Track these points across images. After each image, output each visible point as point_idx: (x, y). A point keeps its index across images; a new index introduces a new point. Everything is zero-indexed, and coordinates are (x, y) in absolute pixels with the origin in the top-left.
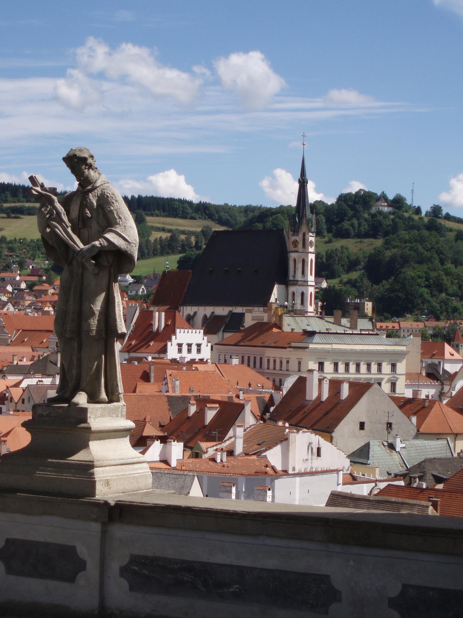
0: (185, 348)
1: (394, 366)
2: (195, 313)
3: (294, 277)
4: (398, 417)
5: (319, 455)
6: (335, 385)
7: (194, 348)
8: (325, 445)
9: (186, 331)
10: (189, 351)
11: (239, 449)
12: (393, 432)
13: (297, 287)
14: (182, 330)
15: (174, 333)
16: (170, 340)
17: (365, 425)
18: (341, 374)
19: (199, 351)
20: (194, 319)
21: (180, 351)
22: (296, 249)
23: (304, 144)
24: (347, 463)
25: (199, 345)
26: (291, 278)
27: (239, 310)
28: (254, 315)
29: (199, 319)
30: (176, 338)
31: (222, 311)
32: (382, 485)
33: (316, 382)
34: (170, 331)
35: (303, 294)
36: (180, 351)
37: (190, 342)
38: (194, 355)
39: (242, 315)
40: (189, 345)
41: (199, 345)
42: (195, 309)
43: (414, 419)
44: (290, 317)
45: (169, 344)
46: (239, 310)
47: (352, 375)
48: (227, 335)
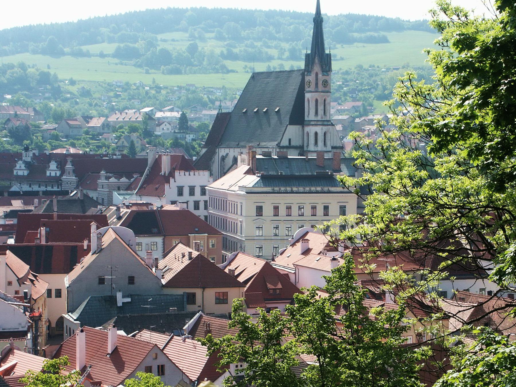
0: (186, 191)
2: (227, 154)
7: (198, 191)
13: (311, 127)
14: (182, 172)
15: (174, 177)
16: (168, 182)
21: (180, 192)
26: (306, 118)
30: (175, 181)
34: (172, 174)
35: (316, 134)
36: (180, 192)
37: (192, 184)
42: (227, 150)
45: (166, 186)
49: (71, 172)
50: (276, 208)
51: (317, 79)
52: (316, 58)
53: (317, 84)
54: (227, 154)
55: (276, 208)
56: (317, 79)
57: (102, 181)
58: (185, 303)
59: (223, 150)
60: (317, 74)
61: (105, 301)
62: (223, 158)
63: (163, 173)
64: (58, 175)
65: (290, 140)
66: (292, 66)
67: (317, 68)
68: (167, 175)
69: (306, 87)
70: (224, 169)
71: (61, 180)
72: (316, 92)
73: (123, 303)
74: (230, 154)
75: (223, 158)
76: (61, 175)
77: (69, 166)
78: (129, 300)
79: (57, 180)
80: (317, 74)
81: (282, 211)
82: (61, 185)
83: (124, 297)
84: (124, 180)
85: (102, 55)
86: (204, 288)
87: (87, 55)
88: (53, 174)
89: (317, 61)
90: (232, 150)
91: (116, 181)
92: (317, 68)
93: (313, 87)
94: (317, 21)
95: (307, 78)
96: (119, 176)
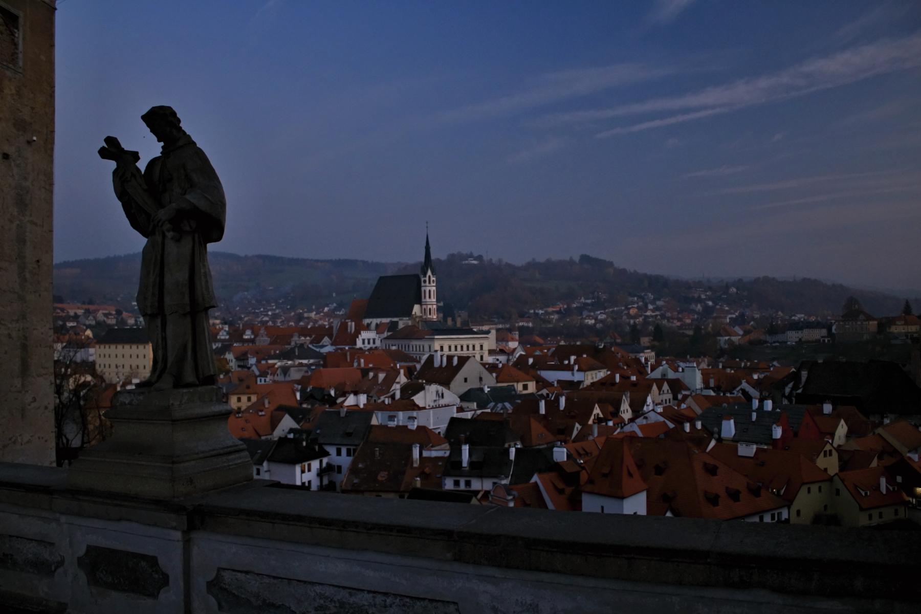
0: (366, 342)
1: (481, 346)
4: (485, 374)
5: (443, 397)
6: (450, 358)
7: (371, 341)
8: (446, 391)
10: (369, 343)
11: (398, 396)
12: (483, 382)
18: (453, 352)
19: (374, 343)
21: (364, 343)
24: (459, 400)
25: (374, 340)
26: (423, 300)
27: (395, 319)
29: (373, 326)
31: (386, 320)
32: (479, 412)
33: (439, 358)
34: (357, 333)
38: (371, 345)
39: (397, 322)
40: (369, 340)
41: (374, 340)
43: (494, 375)
46: (395, 319)
47: (459, 352)
48: (390, 334)
50: (450, 347)
55: (450, 347)
62: (369, 325)
67: (429, 273)
79: (252, 341)
86: (518, 382)
92: (429, 273)
95: (423, 279)
96: (305, 336)
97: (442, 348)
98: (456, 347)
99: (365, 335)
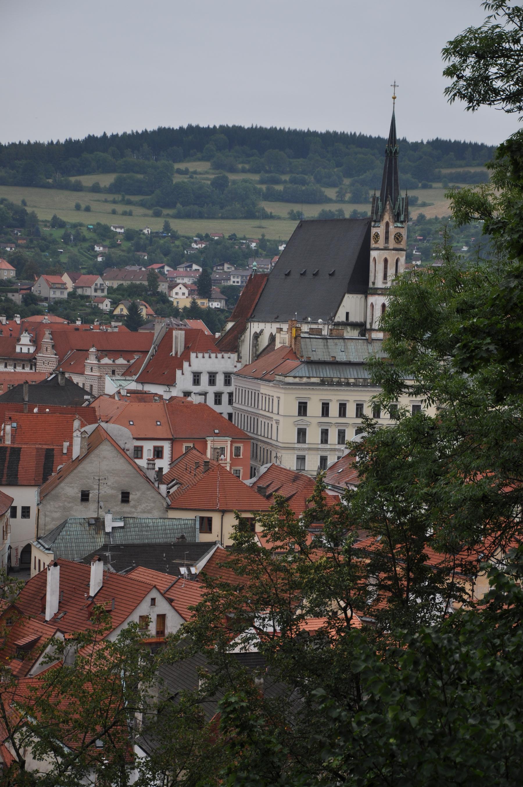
0: (204, 379)
2: (262, 331)
3: (374, 283)
9: (207, 355)
10: (212, 381)
13: (377, 297)
14: (200, 355)
15: (188, 360)
16: (181, 367)
17: (91, 495)
20: (259, 339)
21: (196, 381)
22: (377, 246)
23: (394, 98)
26: (371, 285)
28: (282, 336)
30: (190, 365)
36: (196, 381)
37: (213, 370)
42: (262, 326)
44: (321, 340)
45: (178, 372)
49: (50, 348)
51: (387, 232)
52: (388, 203)
53: (387, 238)
54: (262, 331)
56: (387, 232)
57: (92, 360)
58: (198, 531)
59: (256, 324)
60: (387, 224)
61: (90, 525)
62: (257, 336)
63: (173, 353)
64: (32, 350)
65: (347, 314)
66: (355, 212)
67: (387, 217)
68: (179, 356)
69: (372, 242)
70: (257, 350)
71: (35, 359)
72: (386, 249)
73: (113, 528)
74: (265, 331)
75: (257, 336)
76: (36, 352)
77: (47, 339)
78: (121, 524)
79: (30, 360)
80: (387, 224)
81: (334, 410)
82: (35, 365)
83: (114, 520)
84: (121, 361)
85: (96, 189)
86: (224, 512)
87: (78, 188)
88: (25, 350)
89: (388, 207)
90: (268, 325)
91: (110, 362)
93: (381, 244)
94: (391, 152)
95: (374, 231)
97: (303, 408)
98: (343, 407)
99: (201, 362)
